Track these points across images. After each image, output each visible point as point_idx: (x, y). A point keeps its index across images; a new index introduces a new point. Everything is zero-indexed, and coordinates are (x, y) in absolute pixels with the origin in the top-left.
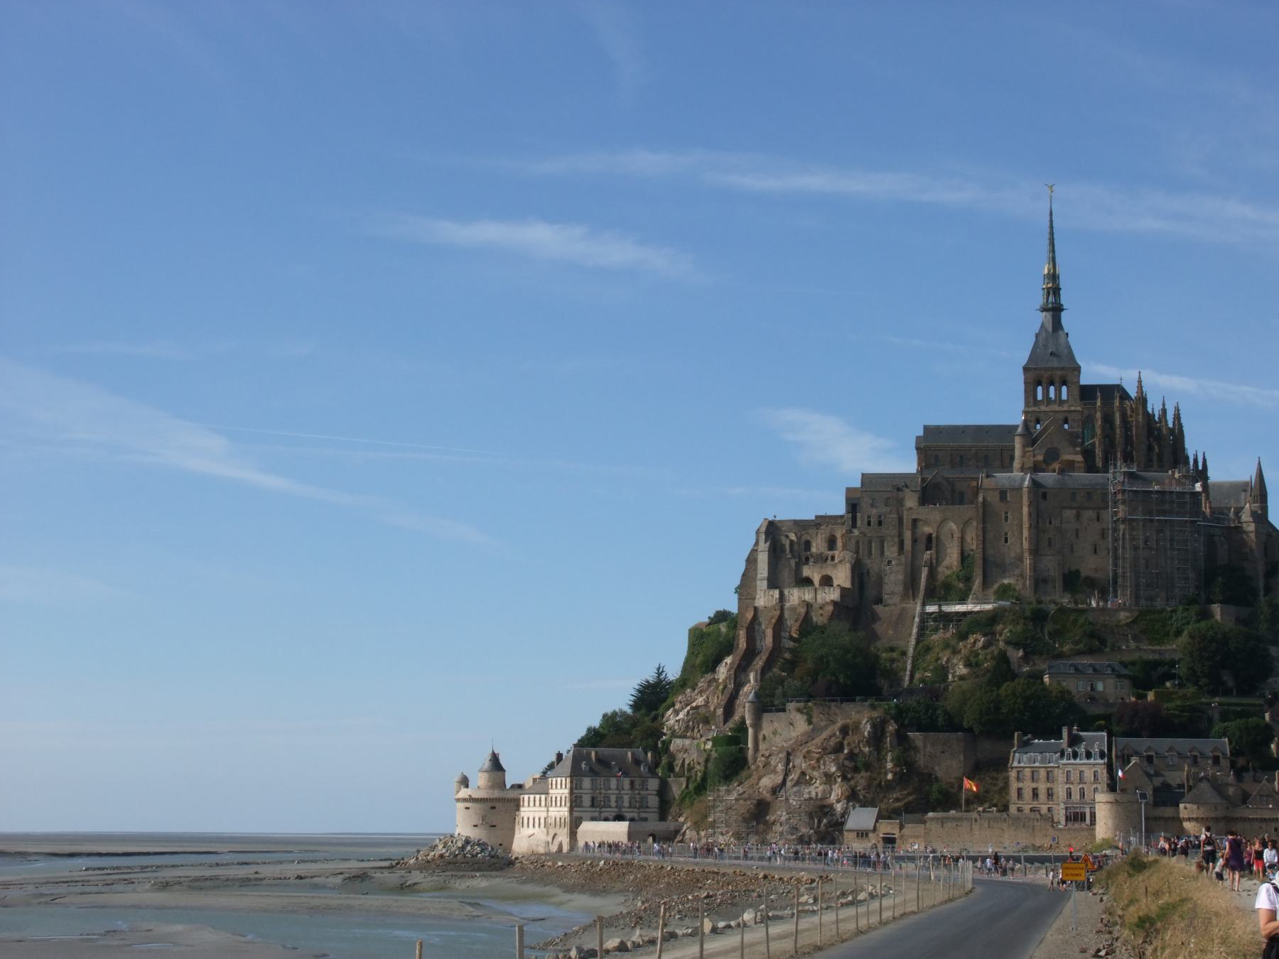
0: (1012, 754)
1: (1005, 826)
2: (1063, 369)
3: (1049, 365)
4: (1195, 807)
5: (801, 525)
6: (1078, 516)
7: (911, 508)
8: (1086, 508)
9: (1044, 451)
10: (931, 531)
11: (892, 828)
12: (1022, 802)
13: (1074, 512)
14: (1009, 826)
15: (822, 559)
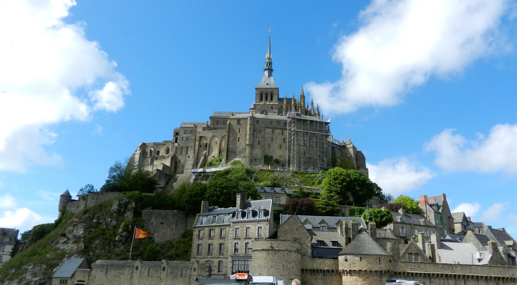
0: (197, 217)
1: (163, 274)
2: (271, 89)
3: (266, 87)
4: (357, 258)
5: (157, 145)
6: (273, 132)
7: (200, 132)
8: (277, 128)
9: (261, 111)
10: (207, 142)
11: (84, 276)
12: (199, 257)
13: (271, 130)
14: (167, 275)
15: (163, 157)
